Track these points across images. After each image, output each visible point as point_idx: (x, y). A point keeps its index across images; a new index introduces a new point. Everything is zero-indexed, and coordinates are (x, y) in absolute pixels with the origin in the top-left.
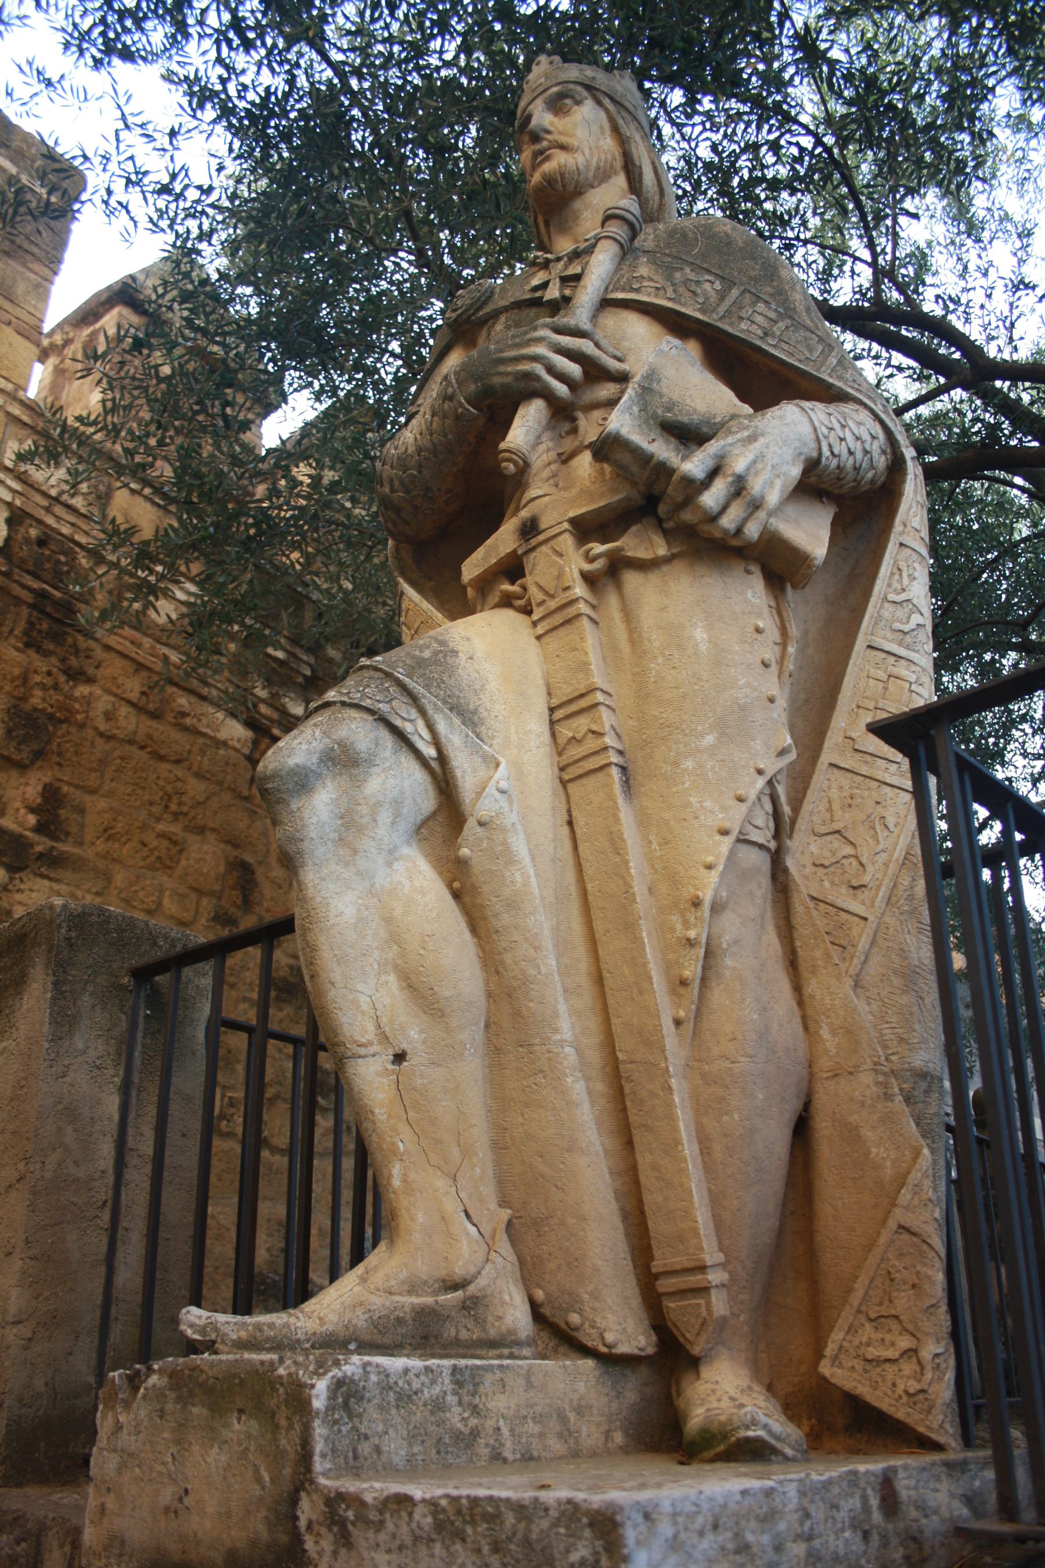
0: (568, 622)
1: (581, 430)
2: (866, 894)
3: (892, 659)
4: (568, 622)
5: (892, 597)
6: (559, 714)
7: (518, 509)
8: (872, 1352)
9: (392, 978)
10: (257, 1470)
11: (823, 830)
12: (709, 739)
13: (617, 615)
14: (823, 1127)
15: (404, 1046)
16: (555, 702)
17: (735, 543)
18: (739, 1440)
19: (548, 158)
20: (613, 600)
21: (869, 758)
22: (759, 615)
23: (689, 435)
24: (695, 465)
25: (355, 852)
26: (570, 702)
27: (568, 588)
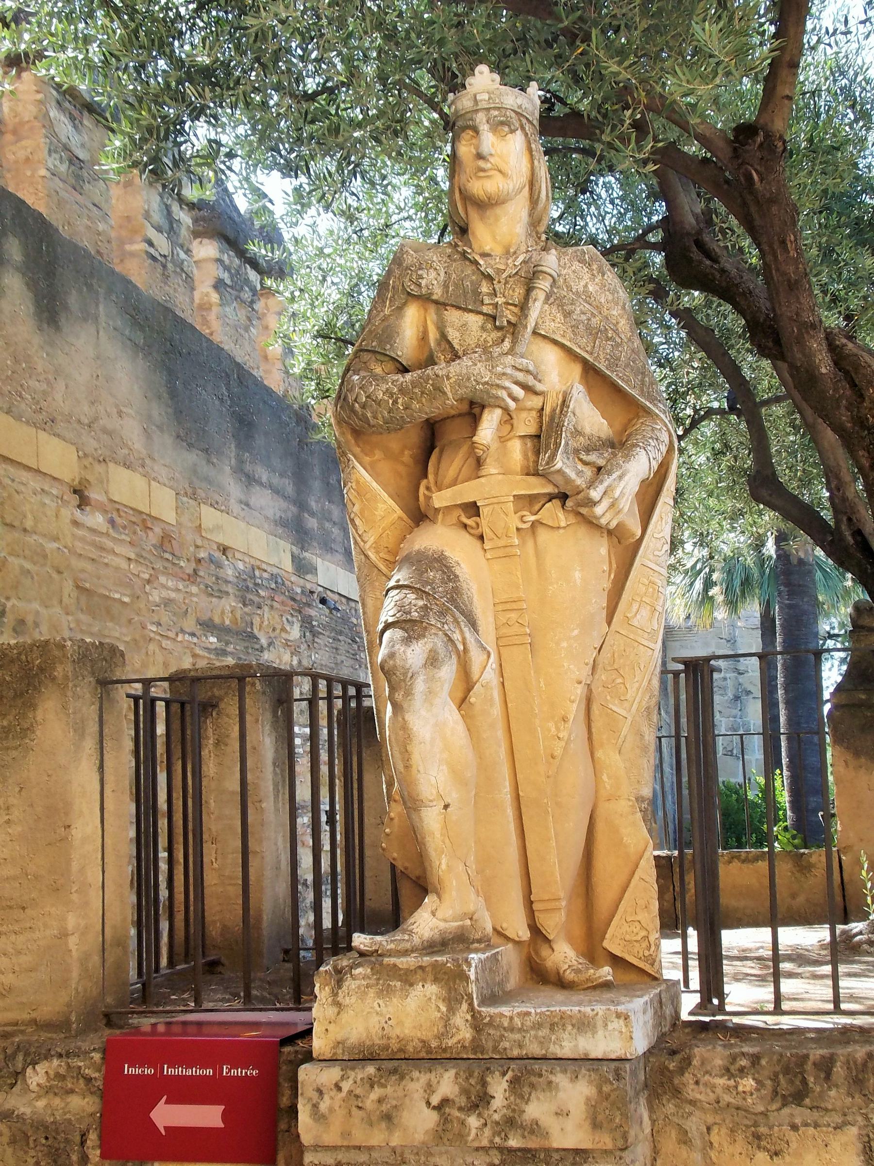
2: (626, 704)
5: (656, 535)
8: (628, 937)
12: (576, 632)
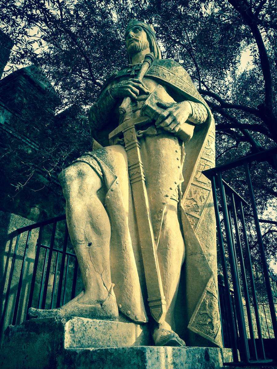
0: (133, 147)
1: (138, 105)
2: (198, 213)
3: (206, 161)
4: (133, 147)
6: (131, 168)
7: (122, 122)
9: (89, 226)
10: (48, 348)
11: (189, 198)
13: (144, 147)
14: (189, 267)
15: (91, 241)
16: (130, 165)
17: (172, 132)
18: (170, 341)
19: (133, 42)
20: (144, 144)
21: (200, 183)
22: (177, 148)
23: (163, 107)
24: (165, 114)
25: (82, 195)
26: (133, 165)
27: (134, 140)
